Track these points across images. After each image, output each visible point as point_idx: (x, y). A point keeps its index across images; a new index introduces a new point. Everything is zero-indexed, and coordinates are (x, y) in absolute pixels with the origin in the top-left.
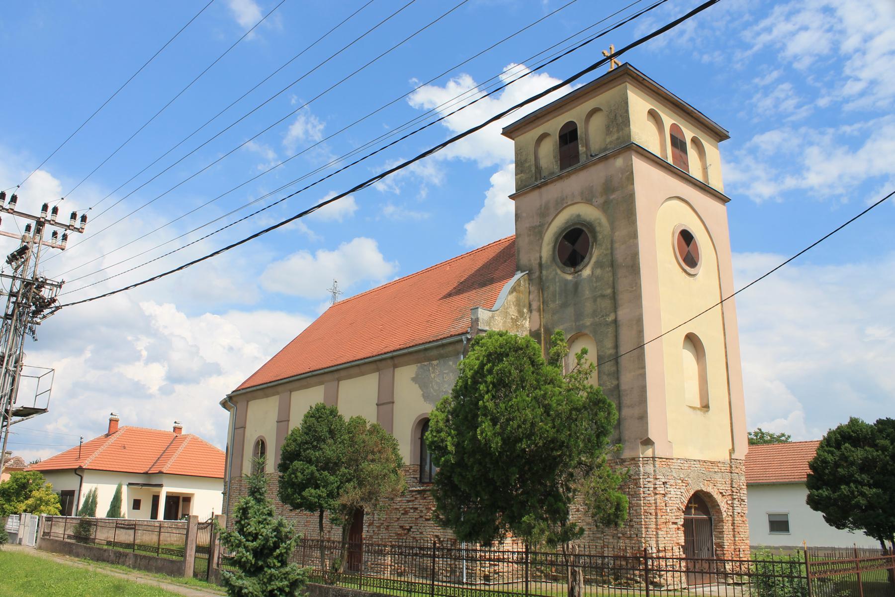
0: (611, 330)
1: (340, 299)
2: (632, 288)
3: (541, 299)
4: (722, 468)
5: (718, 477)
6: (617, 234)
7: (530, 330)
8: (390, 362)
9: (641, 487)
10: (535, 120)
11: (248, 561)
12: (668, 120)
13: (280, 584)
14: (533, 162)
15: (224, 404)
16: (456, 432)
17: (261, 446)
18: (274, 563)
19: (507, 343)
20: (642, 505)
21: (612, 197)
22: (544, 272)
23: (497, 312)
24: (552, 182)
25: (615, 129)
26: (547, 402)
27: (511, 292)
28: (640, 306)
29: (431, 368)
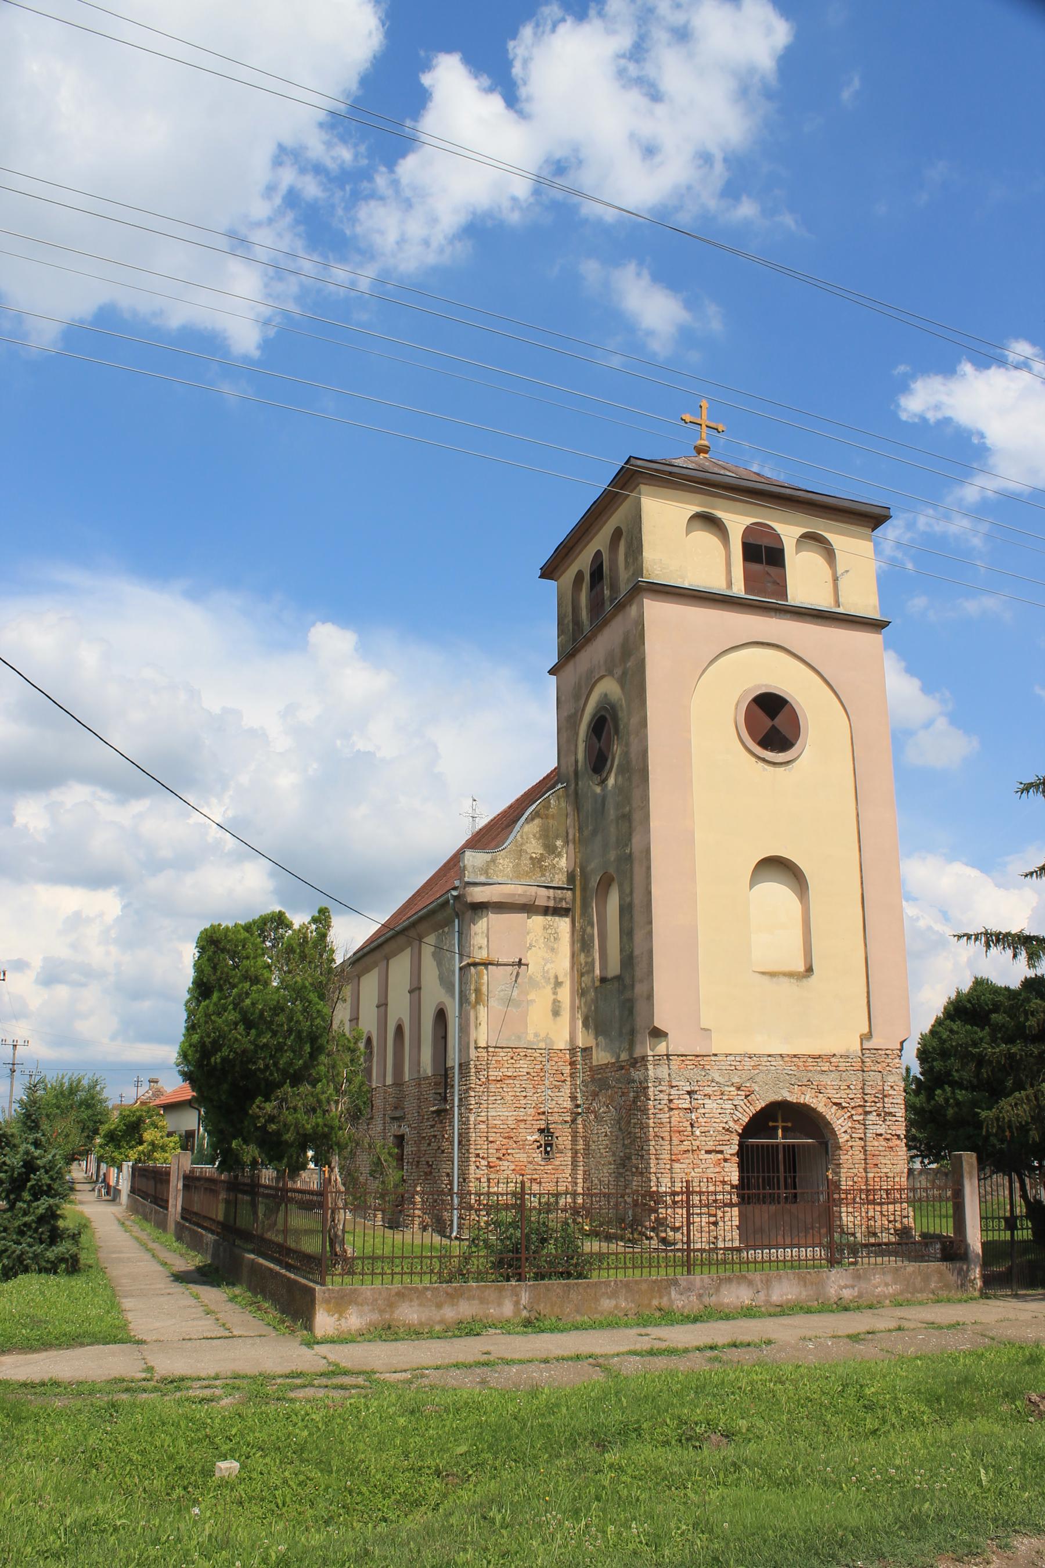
3: (577, 824)
6: (632, 721)
20: (652, 1125)
21: (629, 664)
22: (580, 783)
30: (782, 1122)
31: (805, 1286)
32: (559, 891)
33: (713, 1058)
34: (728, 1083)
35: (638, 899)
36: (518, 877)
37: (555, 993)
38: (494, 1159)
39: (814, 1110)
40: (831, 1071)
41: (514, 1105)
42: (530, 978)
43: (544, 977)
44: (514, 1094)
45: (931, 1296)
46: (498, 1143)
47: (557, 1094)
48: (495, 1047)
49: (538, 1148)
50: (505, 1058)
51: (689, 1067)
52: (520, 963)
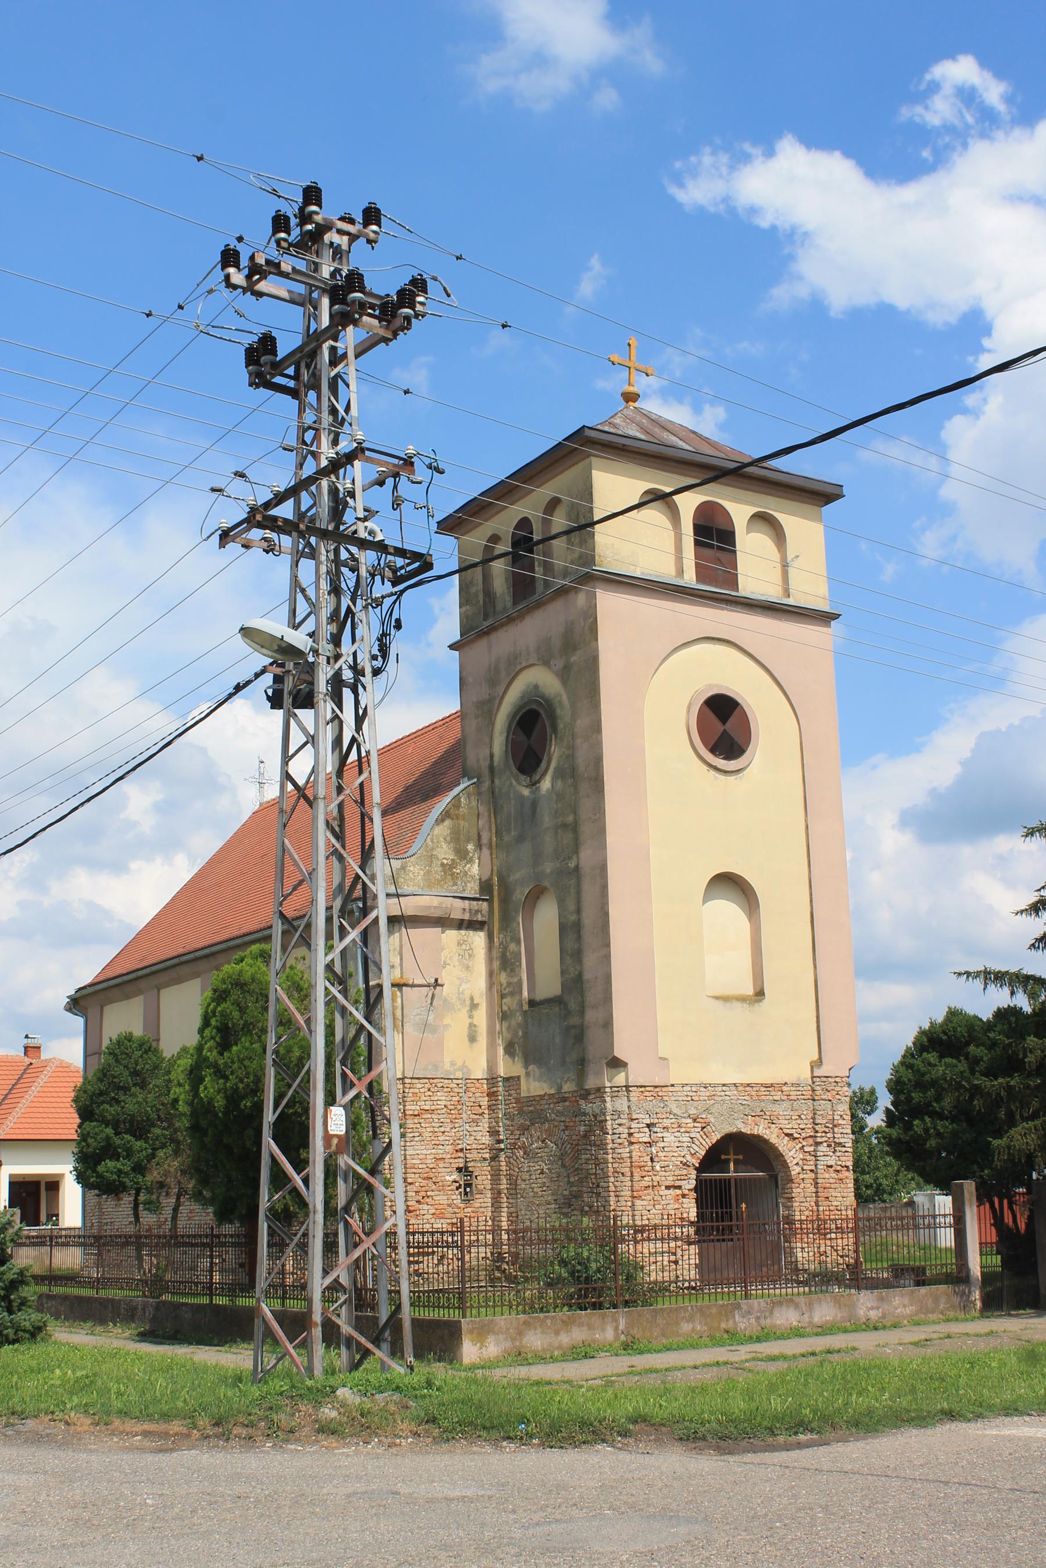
2: (595, 815)
3: (494, 826)
5: (781, 1110)
6: (578, 722)
7: (480, 879)
9: (608, 1134)
14: (480, 587)
20: (611, 1160)
21: (573, 659)
22: (497, 781)
24: (502, 625)
27: (440, 820)
30: (734, 1155)
31: (840, 1308)
32: (475, 903)
33: (671, 1089)
34: (685, 1115)
35: (588, 919)
36: (429, 887)
37: (471, 1017)
38: (414, 1203)
39: (766, 1142)
40: (783, 1101)
41: (433, 1142)
42: (445, 1000)
43: (459, 999)
44: (431, 1129)
45: (941, 1316)
46: (417, 1184)
47: (476, 1129)
48: (411, 1078)
49: (457, 1188)
50: (422, 1090)
51: (648, 1099)
52: (437, 983)
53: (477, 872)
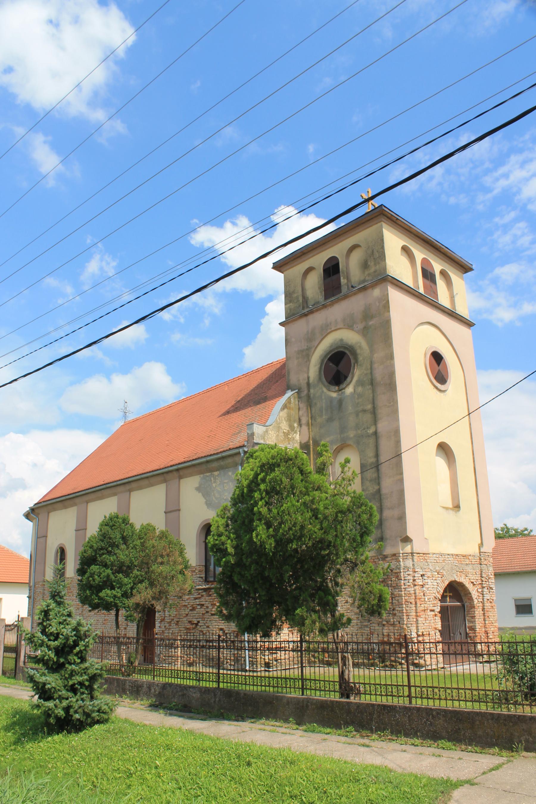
0: (372, 441)
1: (131, 417)
2: (390, 403)
4: (473, 560)
5: (469, 569)
6: (375, 356)
7: (300, 443)
8: (175, 474)
9: (401, 580)
10: (301, 256)
11: (50, 659)
12: (419, 254)
13: (79, 679)
15: (27, 516)
16: (235, 536)
17: (62, 553)
18: (74, 660)
19: (278, 455)
20: (403, 595)
21: (371, 323)
22: (312, 391)
23: (271, 427)
24: (317, 311)
25: (373, 263)
26: (314, 507)
27: (283, 409)
28: (397, 420)
29: (212, 479)
53: (298, 439)
